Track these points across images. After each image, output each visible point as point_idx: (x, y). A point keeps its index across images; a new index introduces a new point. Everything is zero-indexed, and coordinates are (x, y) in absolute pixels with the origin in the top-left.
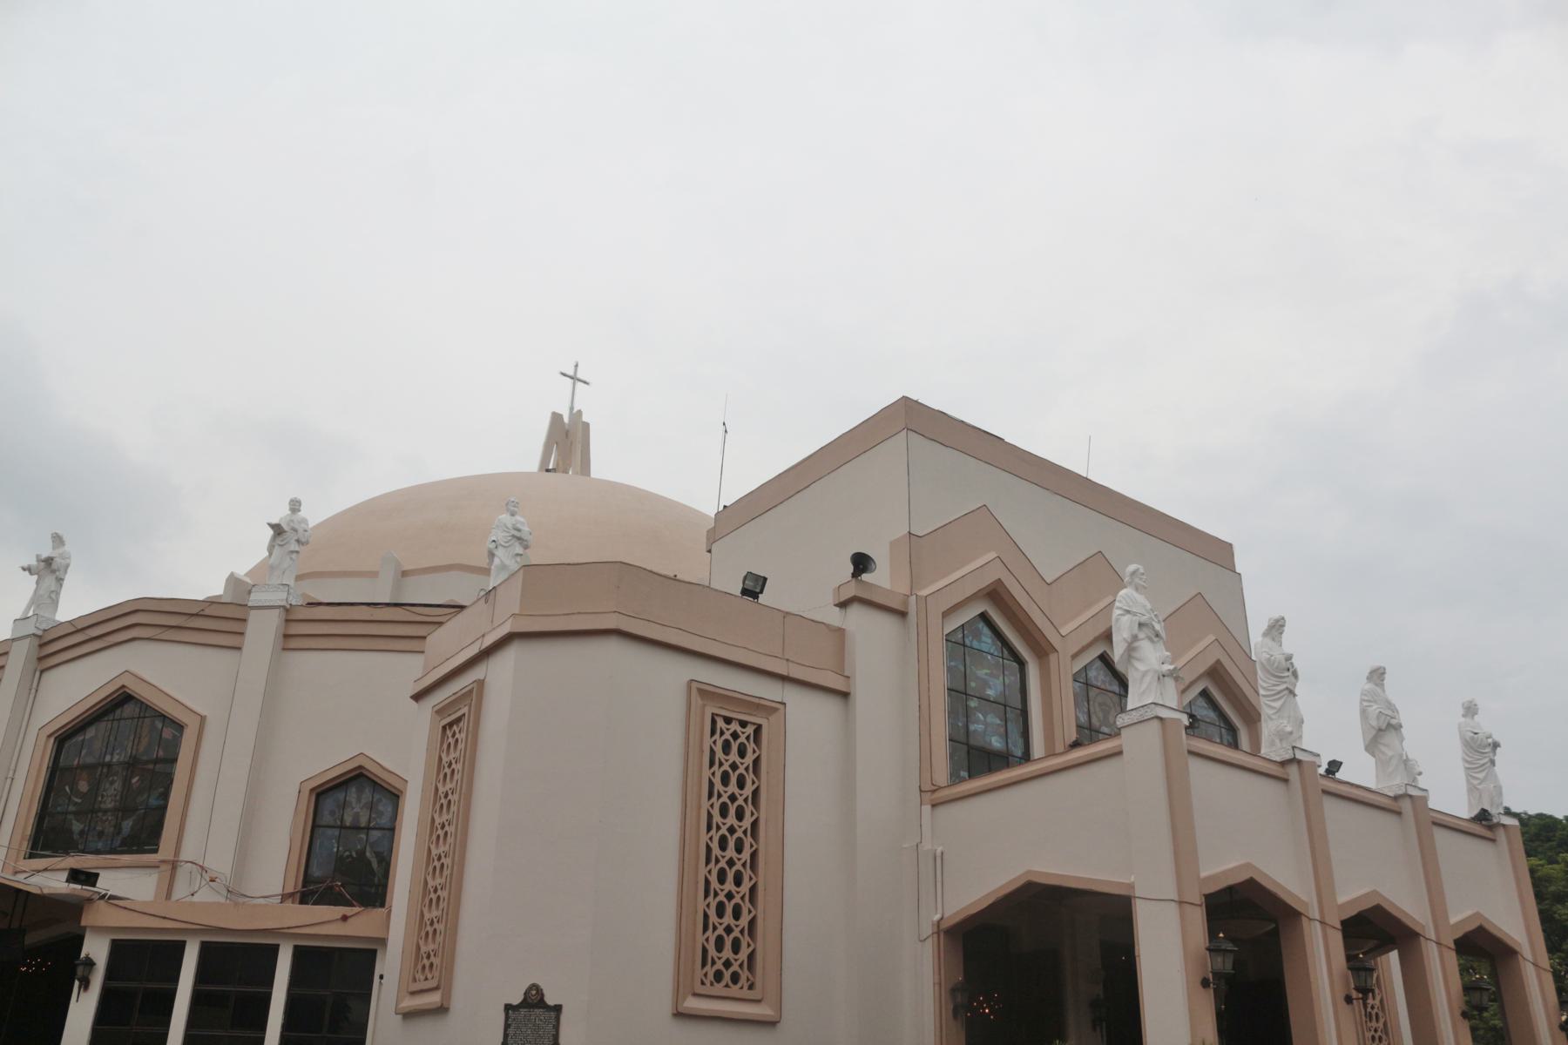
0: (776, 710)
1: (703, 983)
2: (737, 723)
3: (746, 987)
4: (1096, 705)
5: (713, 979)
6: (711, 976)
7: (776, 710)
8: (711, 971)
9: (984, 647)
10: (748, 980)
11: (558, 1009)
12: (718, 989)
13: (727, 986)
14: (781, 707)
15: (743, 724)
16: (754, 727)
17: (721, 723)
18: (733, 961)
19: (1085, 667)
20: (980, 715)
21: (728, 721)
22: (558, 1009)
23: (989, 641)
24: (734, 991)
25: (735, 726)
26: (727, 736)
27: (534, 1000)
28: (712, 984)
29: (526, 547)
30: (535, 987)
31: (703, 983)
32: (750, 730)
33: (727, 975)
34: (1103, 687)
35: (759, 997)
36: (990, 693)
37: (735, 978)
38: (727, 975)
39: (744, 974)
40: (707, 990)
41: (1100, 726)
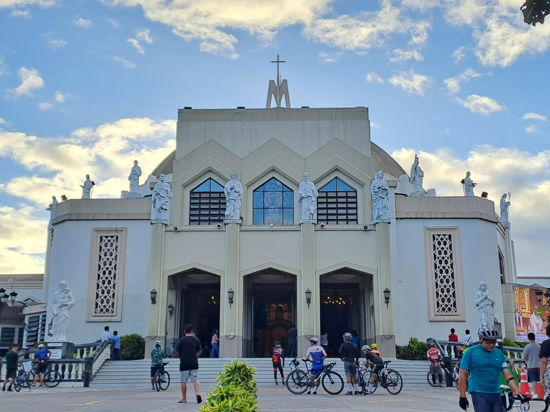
2: (110, 237)
3: (111, 312)
5: (99, 311)
6: (99, 311)
7: (123, 230)
8: (99, 309)
10: (112, 310)
12: (102, 314)
13: (104, 313)
15: (112, 237)
16: (116, 237)
17: (104, 238)
18: (106, 306)
19: (263, 184)
21: (107, 237)
25: (109, 238)
26: (106, 241)
28: (99, 313)
31: (95, 312)
32: (115, 238)
33: (104, 310)
34: (273, 190)
37: (107, 310)
38: (104, 310)
39: (111, 309)
41: (269, 207)
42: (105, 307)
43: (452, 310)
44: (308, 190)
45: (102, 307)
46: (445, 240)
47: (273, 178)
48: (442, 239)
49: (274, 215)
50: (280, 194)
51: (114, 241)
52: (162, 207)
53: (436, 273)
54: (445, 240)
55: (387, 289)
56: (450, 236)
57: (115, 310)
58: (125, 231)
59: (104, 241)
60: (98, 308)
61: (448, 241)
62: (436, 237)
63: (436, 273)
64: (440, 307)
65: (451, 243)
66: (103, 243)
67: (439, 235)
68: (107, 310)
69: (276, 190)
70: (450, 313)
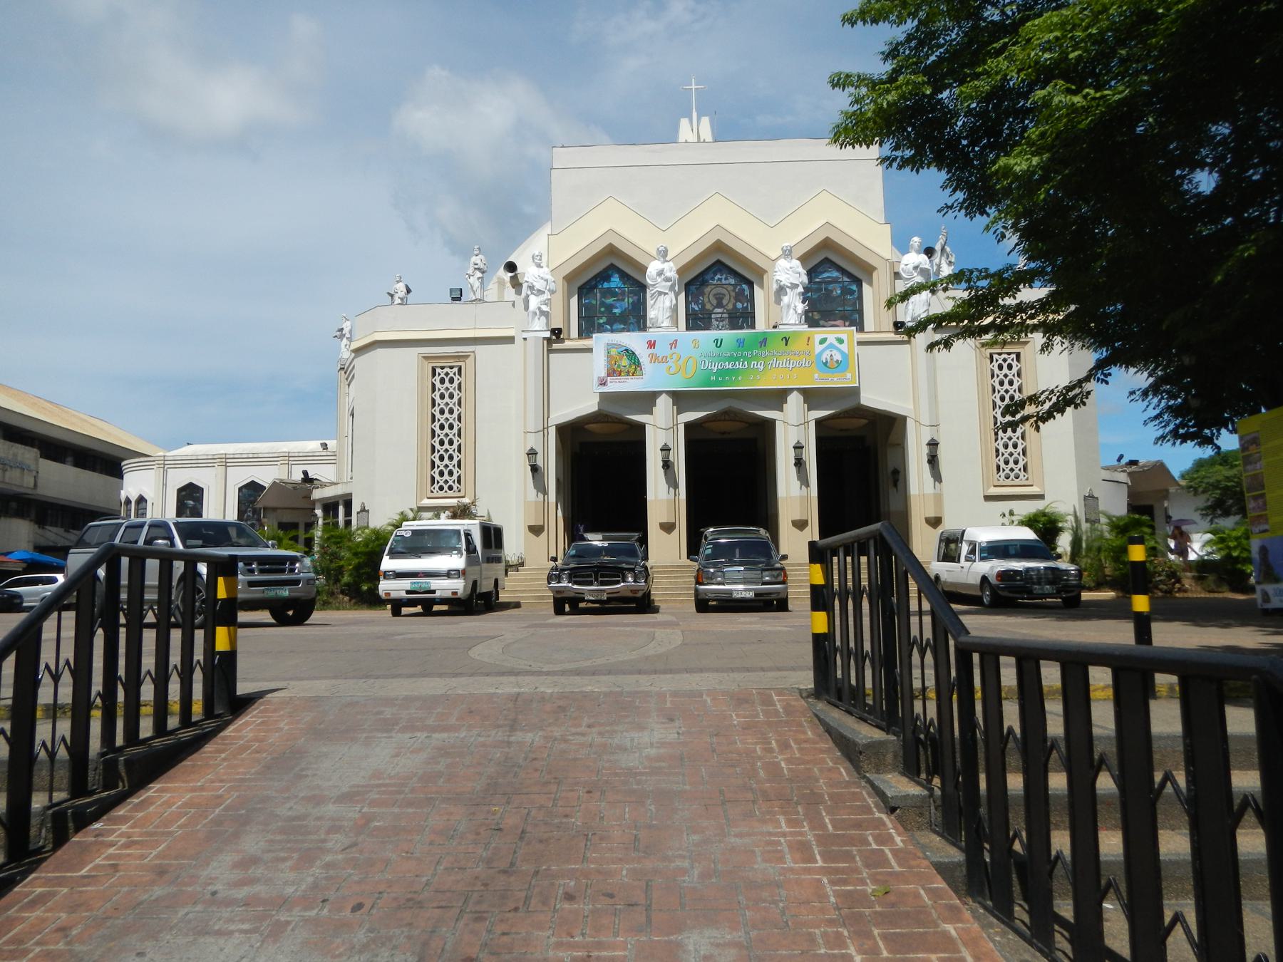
0: (468, 356)
1: (432, 492)
4: (711, 297)
7: (468, 356)
8: (436, 486)
9: (613, 285)
11: (368, 511)
12: (442, 493)
14: (472, 354)
15: (451, 368)
17: (438, 370)
20: (608, 327)
22: (368, 511)
23: (618, 280)
24: (450, 493)
25: (447, 370)
27: (363, 510)
29: (483, 272)
30: (363, 503)
32: (456, 370)
33: (446, 487)
34: (719, 282)
35: (463, 495)
36: (616, 311)
37: (451, 488)
38: (446, 487)
39: (455, 486)
40: (435, 494)
42: (446, 482)
43: (1021, 477)
44: (790, 272)
45: (441, 483)
46: (1009, 361)
47: (719, 262)
48: (1005, 360)
49: (721, 324)
50: (731, 288)
51: (455, 374)
52: (539, 308)
53: (994, 417)
54: (1009, 361)
55: (932, 439)
56: (1018, 355)
57: (462, 487)
58: (472, 358)
59: (439, 374)
60: (436, 486)
61: (1015, 363)
62: (995, 356)
63: (994, 417)
64: (1001, 473)
65: (1019, 366)
66: (437, 378)
67: (1000, 354)
68: (451, 488)
69: (724, 282)
70: (1017, 482)
